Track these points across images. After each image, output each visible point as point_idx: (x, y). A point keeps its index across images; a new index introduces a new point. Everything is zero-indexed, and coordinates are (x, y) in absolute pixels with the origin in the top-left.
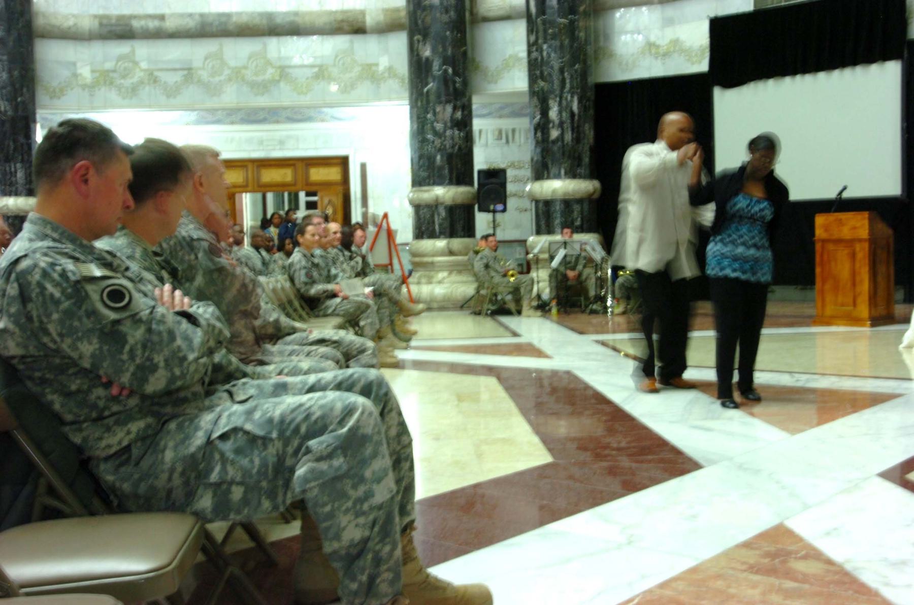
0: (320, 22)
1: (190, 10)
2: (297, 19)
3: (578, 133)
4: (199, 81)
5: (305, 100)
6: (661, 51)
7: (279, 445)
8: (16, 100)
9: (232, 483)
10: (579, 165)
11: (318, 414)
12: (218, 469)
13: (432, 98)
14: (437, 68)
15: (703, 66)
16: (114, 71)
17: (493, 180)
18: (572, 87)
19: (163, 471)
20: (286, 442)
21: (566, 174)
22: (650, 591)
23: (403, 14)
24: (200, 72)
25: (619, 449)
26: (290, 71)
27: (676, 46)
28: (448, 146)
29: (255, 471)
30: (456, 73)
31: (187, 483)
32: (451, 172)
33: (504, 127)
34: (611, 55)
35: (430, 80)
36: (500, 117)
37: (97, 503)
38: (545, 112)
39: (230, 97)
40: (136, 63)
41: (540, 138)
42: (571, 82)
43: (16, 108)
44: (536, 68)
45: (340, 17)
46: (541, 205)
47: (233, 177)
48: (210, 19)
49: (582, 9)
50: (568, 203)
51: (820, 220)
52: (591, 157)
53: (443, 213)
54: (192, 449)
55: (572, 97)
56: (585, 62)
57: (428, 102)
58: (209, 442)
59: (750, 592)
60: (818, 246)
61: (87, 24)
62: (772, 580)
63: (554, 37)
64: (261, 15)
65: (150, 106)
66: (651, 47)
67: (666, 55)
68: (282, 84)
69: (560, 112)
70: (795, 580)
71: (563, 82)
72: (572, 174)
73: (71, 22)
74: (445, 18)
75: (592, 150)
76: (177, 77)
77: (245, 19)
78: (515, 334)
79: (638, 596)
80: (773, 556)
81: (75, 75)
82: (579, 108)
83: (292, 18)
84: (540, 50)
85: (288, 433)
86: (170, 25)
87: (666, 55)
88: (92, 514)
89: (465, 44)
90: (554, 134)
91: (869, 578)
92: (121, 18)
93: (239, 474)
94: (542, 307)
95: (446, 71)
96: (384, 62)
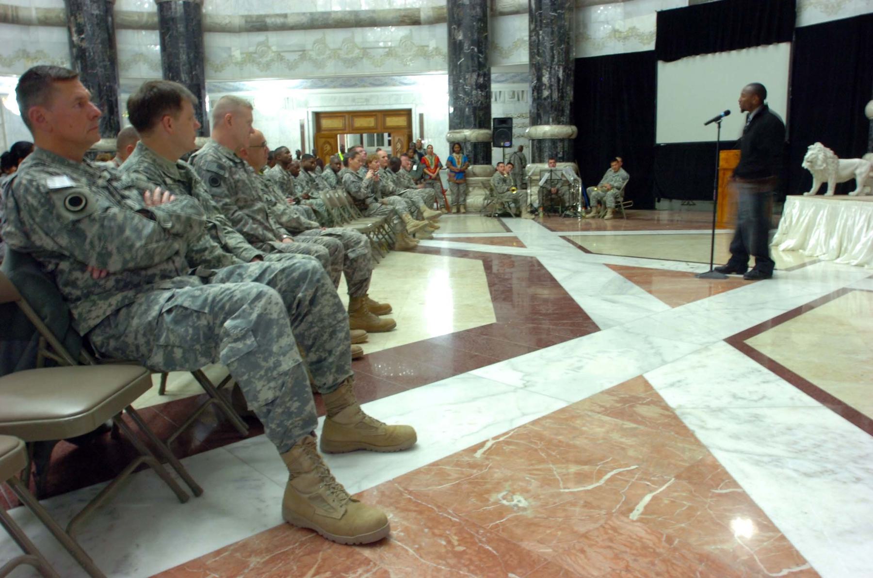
0: (390, 17)
1: (304, 11)
2: (375, 15)
3: (562, 93)
4: (310, 59)
5: (379, 71)
6: (622, 35)
7: (210, 318)
8: (191, 72)
9: (173, 346)
10: (562, 115)
11: (239, 296)
12: (164, 335)
13: (464, 68)
15: (651, 46)
16: (255, 53)
17: (504, 125)
18: (559, 61)
19: (130, 332)
20: (216, 317)
21: (553, 121)
22: (524, 426)
23: (445, 10)
24: (311, 53)
25: (545, 315)
26: (368, 51)
27: (633, 32)
29: (188, 338)
30: (480, 51)
31: (148, 343)
32: (475, 120)
33: (516, 90)
34: (588, 38)
35: (462, 56)
36: (514, 82)
37: (85, 355)
38: (539, 79)
39: (331, 69)
40: (269, 47)
43: (192, 79)
44: (535, 48)
45: (403, 13)
46: (535, 142)
47: (336, 123)
48: (317, 17)
49: (567, 5)
50: (554, 141)
51: (723, 155)
52: (571, 110)
53: (470, 148)
54: (150, 318)
56: (568, 43)
57: (460, 72)
58: (161, 314)
59: (598, 430)
60: (721, 174)
61: (237, 22)
62: (620, 422)
63: (547, 25)
64: (350, 12)
65: (278, 76)
67: (626, 38)
68: (364, 60)
69: (550, 78)
70: (635, 421)
71: (553, 57)
72: (558, 122)
73: (227, 21)
75: (571, 104)
77: (340, 16)
78: (508, 230)
79: (513, 430)
80: (624, 401)
81: (230, 56)
83: (371, 14)
84: (538, 35)
85: (216, 309)
86: (291, 21)
87: (626, 38)
88: (80, 363)
89: (487, 31)
90: (546, 93)
91: (690, 422)
92: (259, 17)
93: (178, 340)
94: (534, 212)
96: (432, 45)
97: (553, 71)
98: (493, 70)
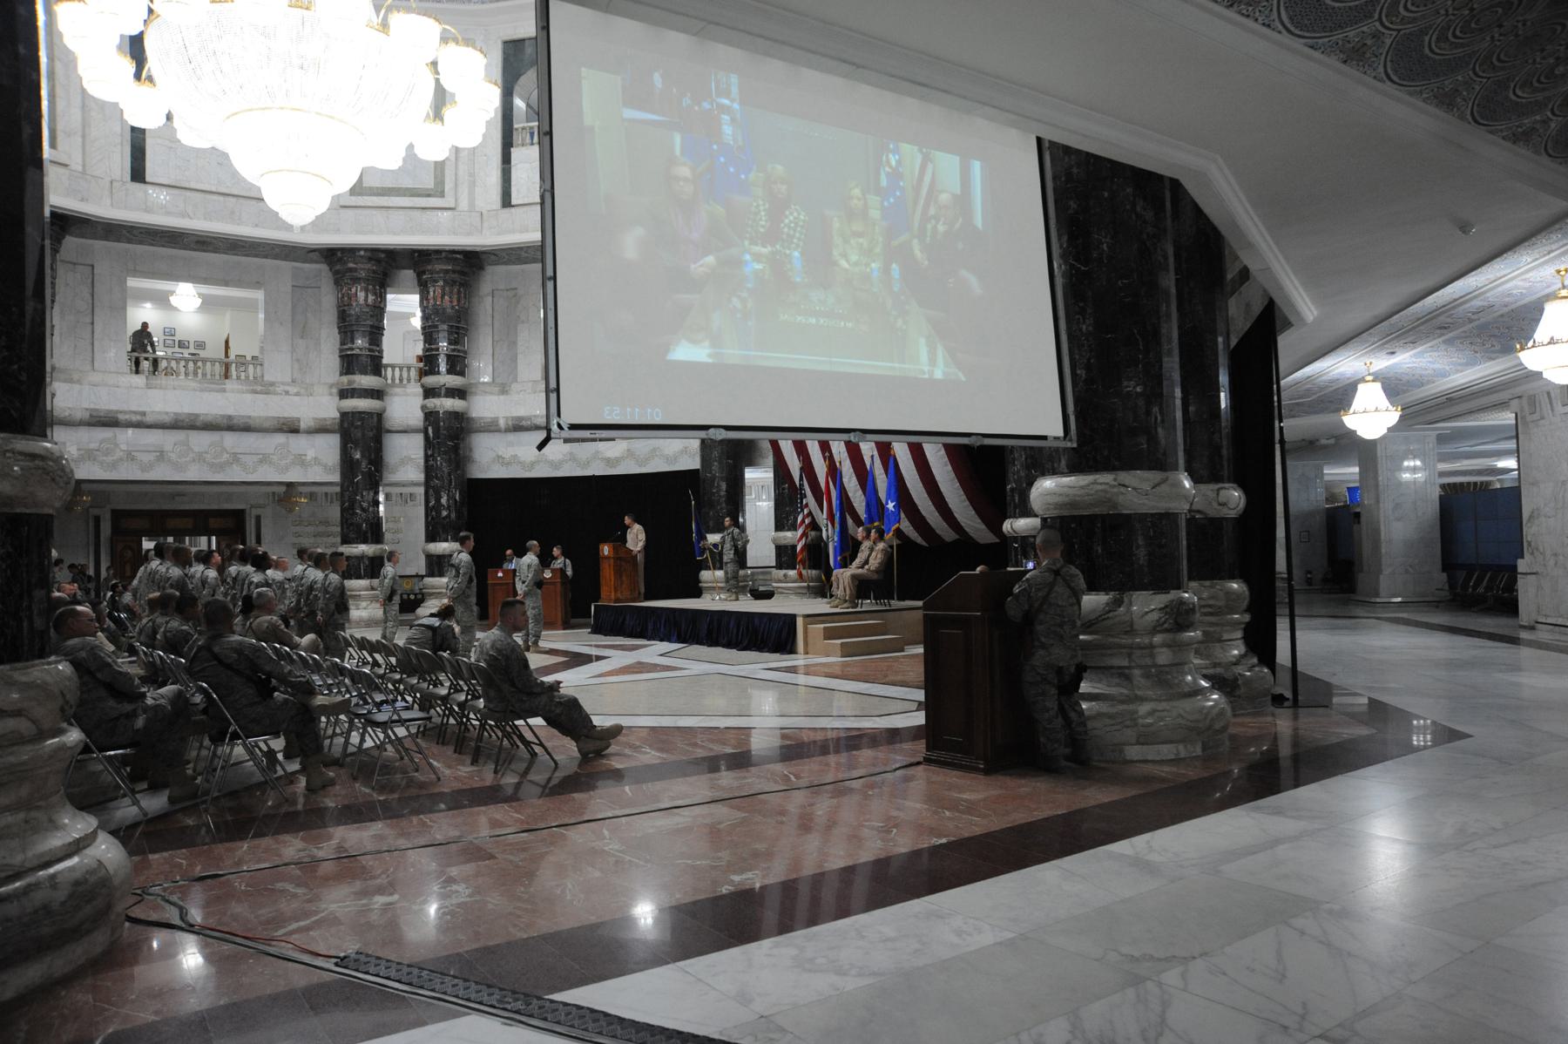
0: (267, 425)
2: (251, 422)
38: (438, 500)
40: (117, 445)
44: (429, 470)
61: (79, 415)
63: (445, 453)
66: (499, 459)
74: (371, 434)
76: (152, 457)
77: (209, 418)
86: (149, 419)
90: (445, 513)
96: (311, 454)
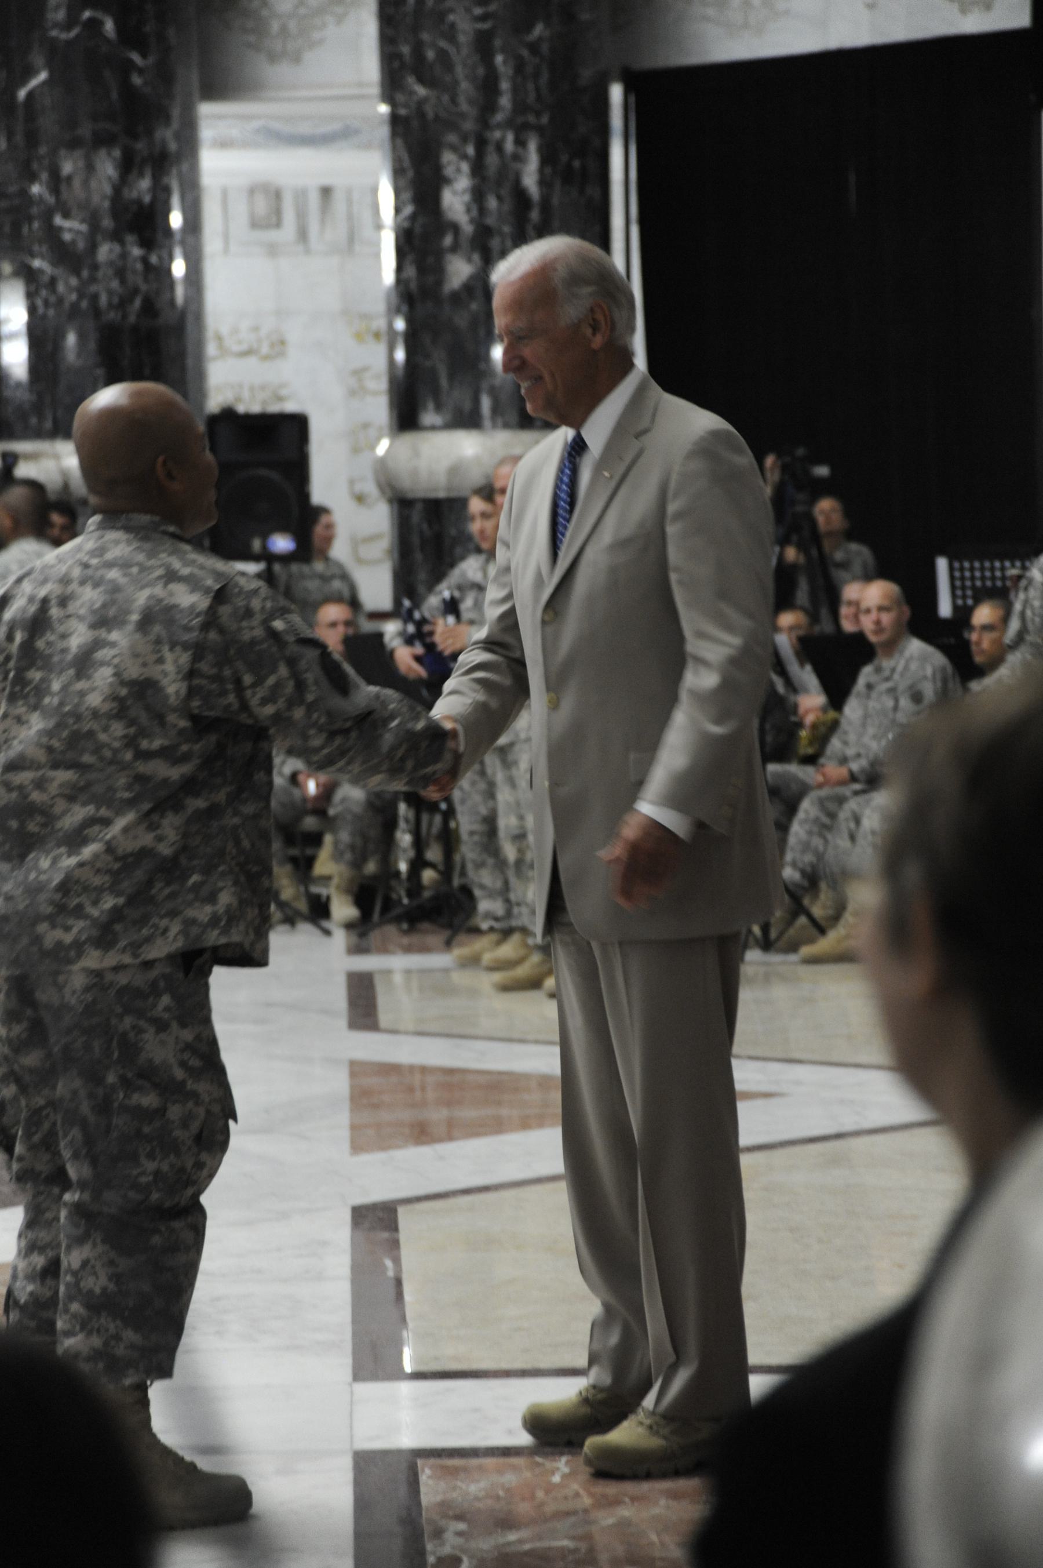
13: (48, 123)
14: (61, 15)
18: (520, 106)
21: (495, 411)
28: (103, 300)
35: (38, 58)
41: (413, 286)
42: (515, 90)
46: (416, 516)
55: (520, 142)
57: (32, 139)
69: (478, 195)
71: (489, 87)
82: (543, 182)
95: (94, 25)
97: (492, 160)
98: (214, 119)
